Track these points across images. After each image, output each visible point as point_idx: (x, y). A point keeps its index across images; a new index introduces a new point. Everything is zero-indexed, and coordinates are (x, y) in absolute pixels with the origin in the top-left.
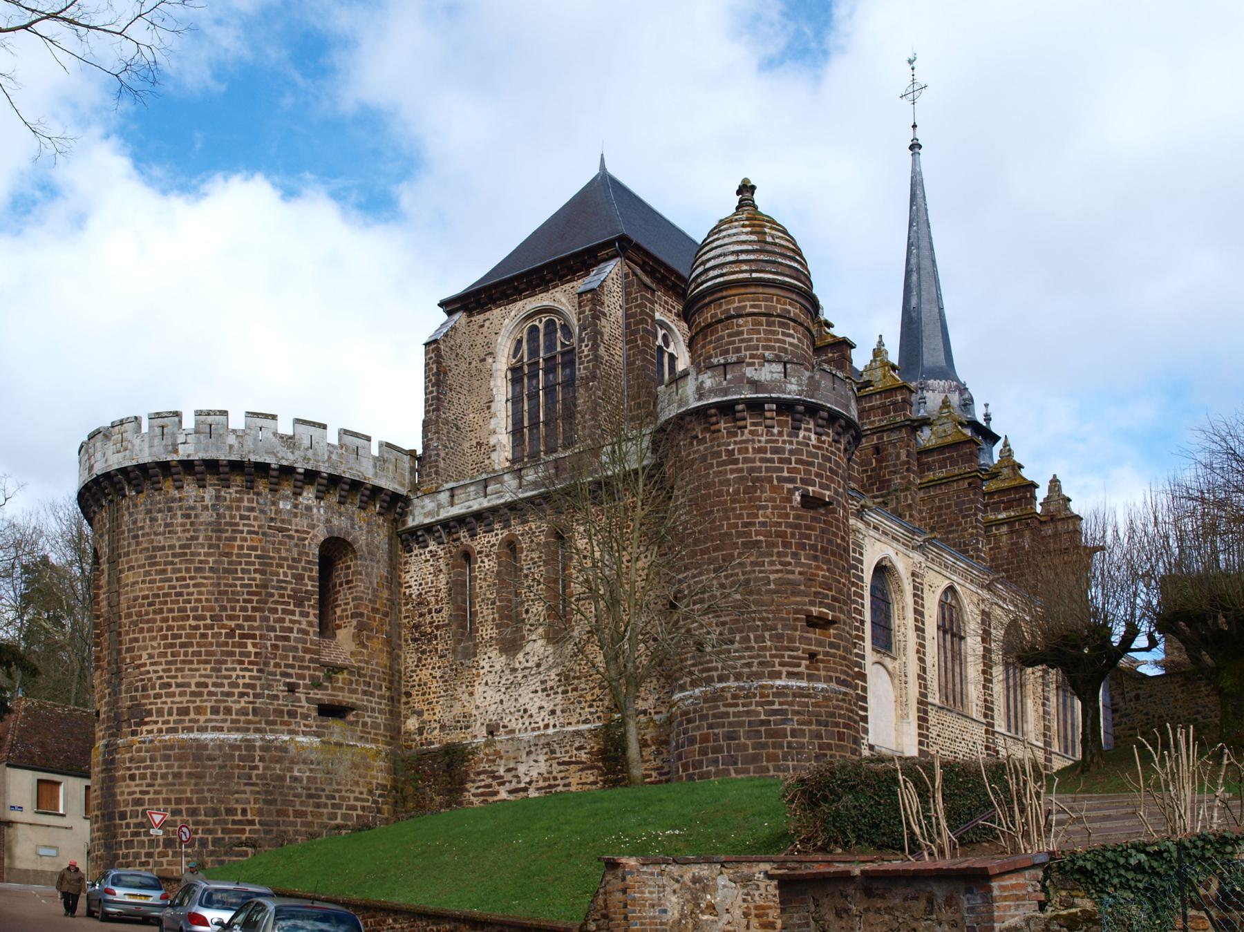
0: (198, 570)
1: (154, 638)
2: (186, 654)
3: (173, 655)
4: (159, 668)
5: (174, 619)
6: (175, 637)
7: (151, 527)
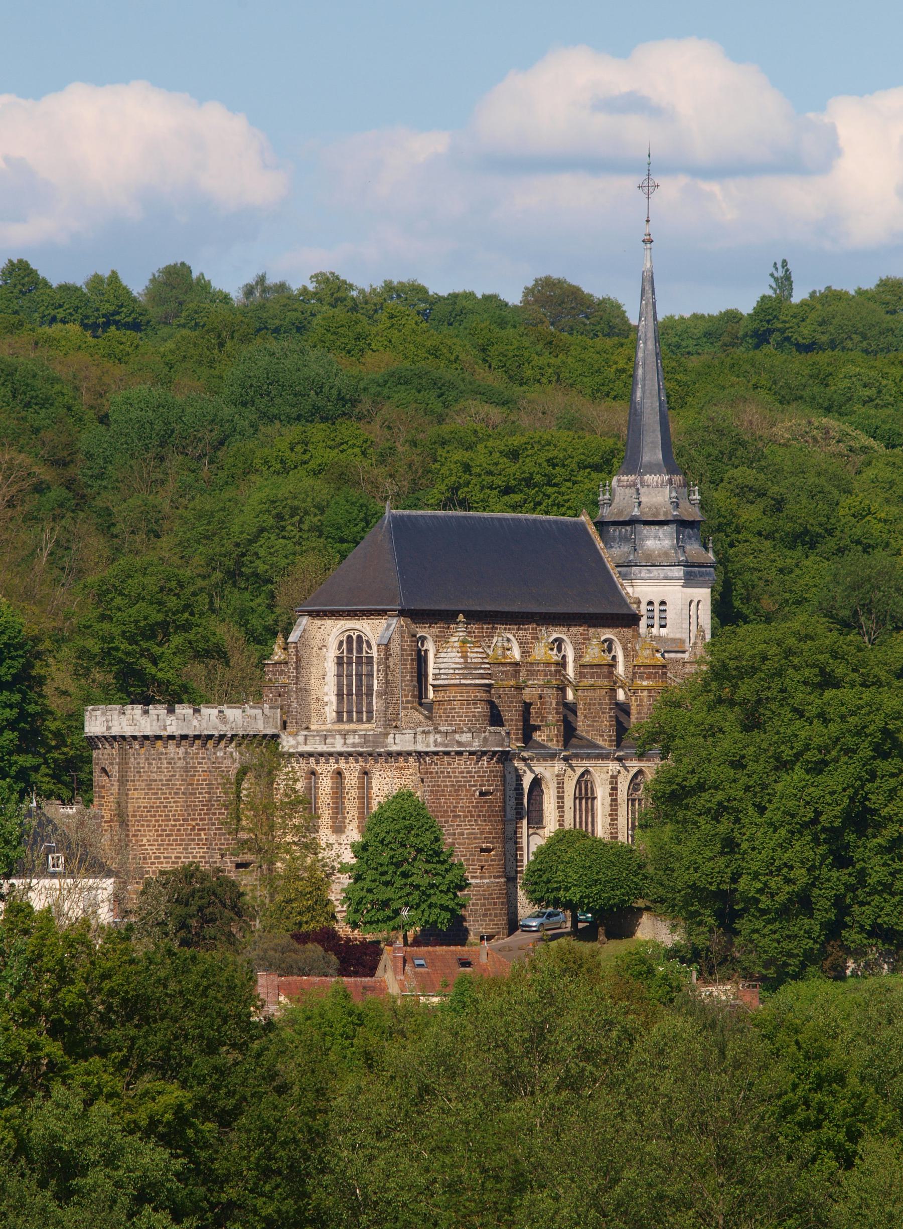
0: (176, 793)
1: (151, 831)
2: (169, 840)
3: (162, 840)
4: (154, 848)
5: (162, 821)
6: (163, 830)
7: (149, 768)
